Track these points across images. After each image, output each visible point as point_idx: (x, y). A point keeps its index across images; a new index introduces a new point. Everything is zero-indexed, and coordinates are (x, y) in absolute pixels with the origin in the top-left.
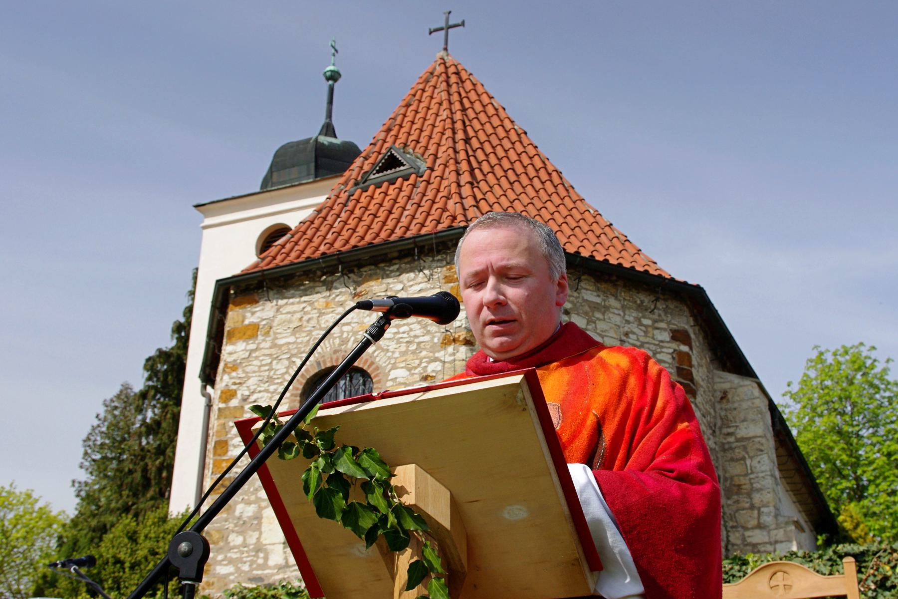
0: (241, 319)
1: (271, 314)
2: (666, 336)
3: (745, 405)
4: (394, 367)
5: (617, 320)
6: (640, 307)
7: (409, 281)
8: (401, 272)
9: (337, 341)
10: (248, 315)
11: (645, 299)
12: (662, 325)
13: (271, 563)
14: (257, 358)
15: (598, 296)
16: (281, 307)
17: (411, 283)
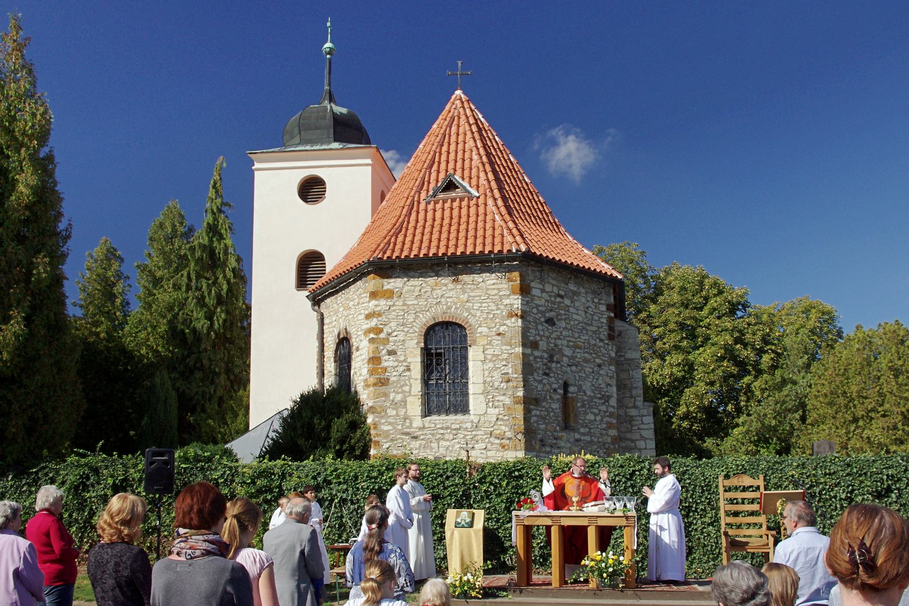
2: (603, 308)
3: (631, 341)
4: (480, 326)
5: (583, 300)
6: (594, 292)
8: (482, 271)
9: (445, 307)
11: (594, 286)
12: (602, 302)
13: (414, 425)
14: (394, 310)
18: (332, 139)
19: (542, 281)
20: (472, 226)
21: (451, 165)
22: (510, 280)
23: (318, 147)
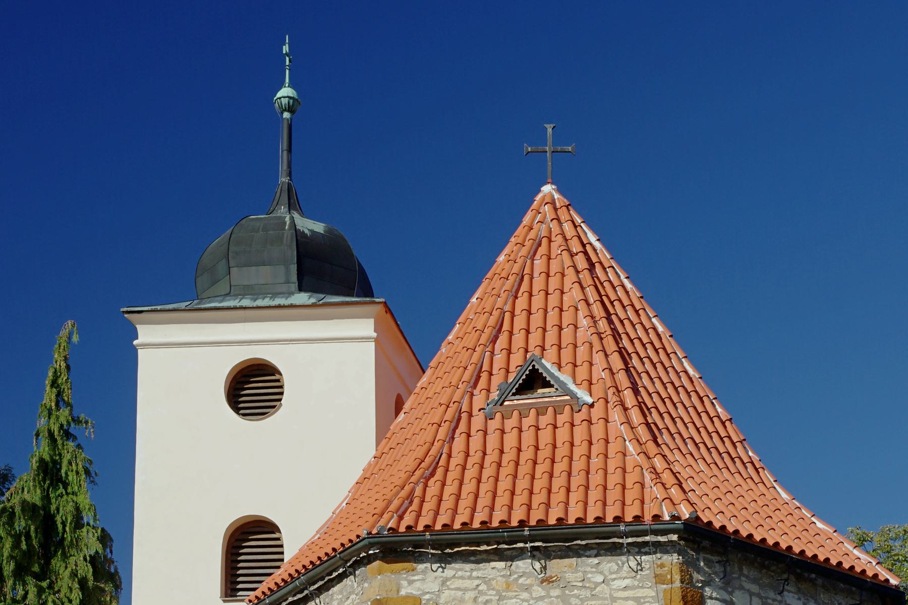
0: (395, 588)
1: (435, 587)
7: (611, 573)
10: (405, 583)
15: (799, 599)
16: (447, 579)
17: (614, 576)
18: (294, 286)
19: (727, 584)
20: (579, 464)
21: (535, 339)
22: (659, 579)
23: (267, 302)
